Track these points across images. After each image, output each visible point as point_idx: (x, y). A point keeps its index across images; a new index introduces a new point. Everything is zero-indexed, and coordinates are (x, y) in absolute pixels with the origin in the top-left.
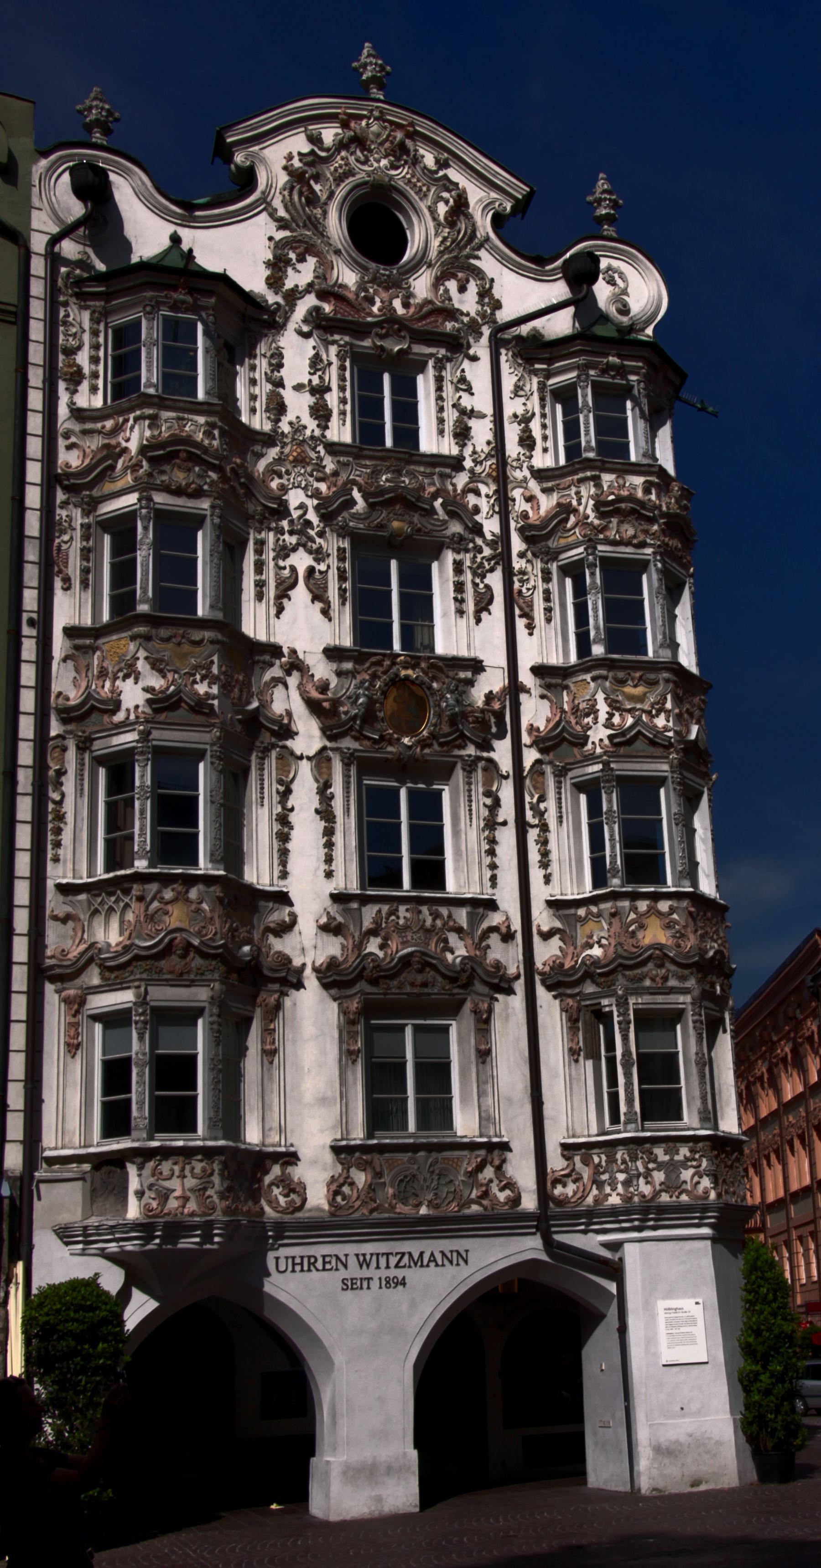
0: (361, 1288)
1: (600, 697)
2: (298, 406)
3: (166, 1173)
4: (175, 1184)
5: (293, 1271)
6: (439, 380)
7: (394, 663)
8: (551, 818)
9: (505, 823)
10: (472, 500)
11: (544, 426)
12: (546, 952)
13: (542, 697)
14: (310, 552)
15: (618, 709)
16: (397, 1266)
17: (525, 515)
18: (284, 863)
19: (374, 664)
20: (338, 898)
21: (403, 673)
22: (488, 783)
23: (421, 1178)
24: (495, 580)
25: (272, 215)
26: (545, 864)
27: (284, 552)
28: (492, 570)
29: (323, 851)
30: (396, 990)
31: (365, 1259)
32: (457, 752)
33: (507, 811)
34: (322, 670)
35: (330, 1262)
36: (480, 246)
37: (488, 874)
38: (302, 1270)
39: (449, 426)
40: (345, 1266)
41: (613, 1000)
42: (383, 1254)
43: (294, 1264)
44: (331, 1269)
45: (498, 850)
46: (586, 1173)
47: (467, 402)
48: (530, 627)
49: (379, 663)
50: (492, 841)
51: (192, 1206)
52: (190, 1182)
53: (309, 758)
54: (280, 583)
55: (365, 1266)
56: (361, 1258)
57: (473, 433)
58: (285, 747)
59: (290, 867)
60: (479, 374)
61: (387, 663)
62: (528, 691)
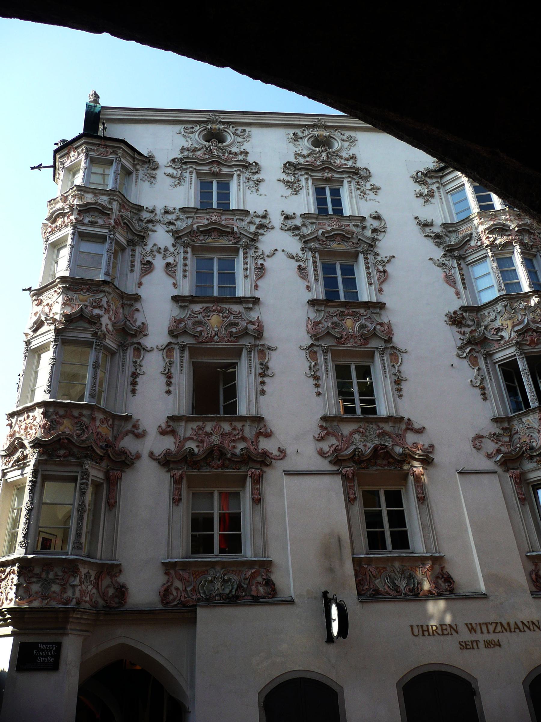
0: (473, 648)
5: (423, 635)
16: (494, 632)
31: (472, 628)
35: (446, 629)
38: (429, 635)
40: (457, 632)
42: (483, 623)
43: (423, 631)
44: (448, 634)
55: (473, 632)
56: (470, 627)
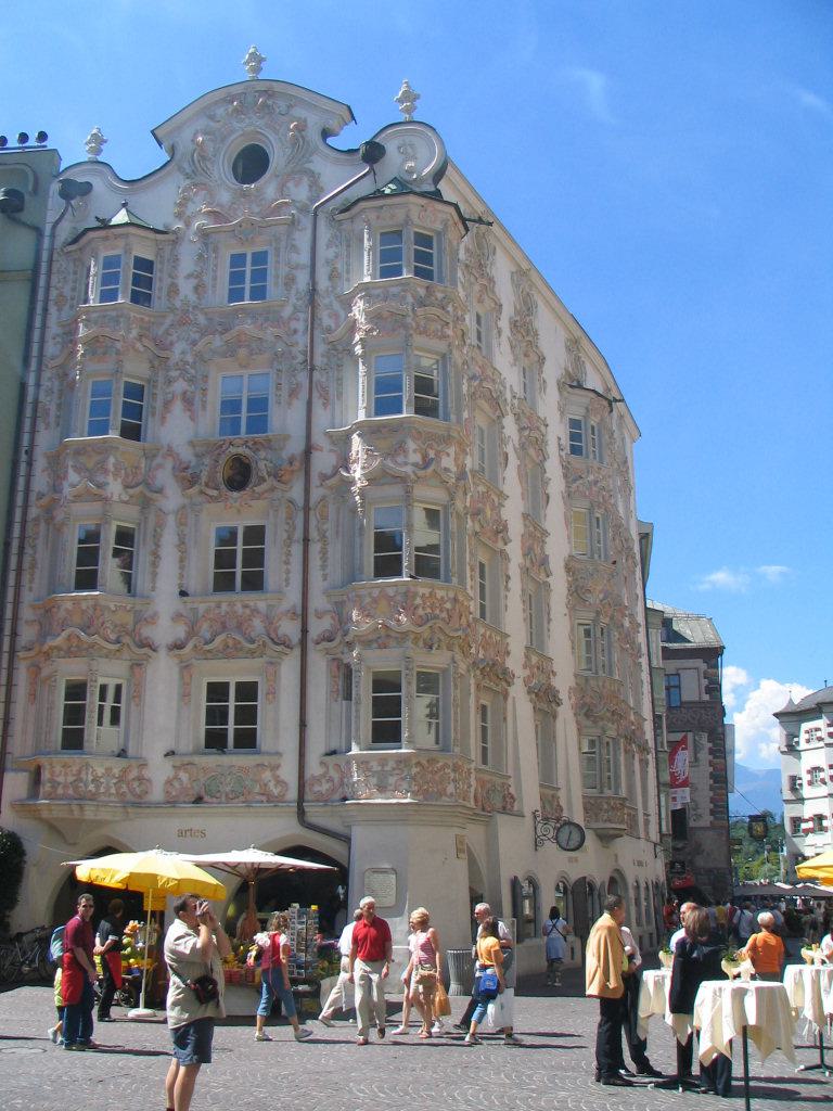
2: (186, 288)
3: (58, 772)
4: (61, 779)
10: (294, 325)
13: (331, 451)
17: (329, 330)
24: (302, 377)
25: (180, 169)
26: (323, 567)
27: (169, 382)
33: (299, 534)
36: (312, 154)
37: (285, 576)
51: (71, 792)
52: (71, 779)
59: (157, 585)
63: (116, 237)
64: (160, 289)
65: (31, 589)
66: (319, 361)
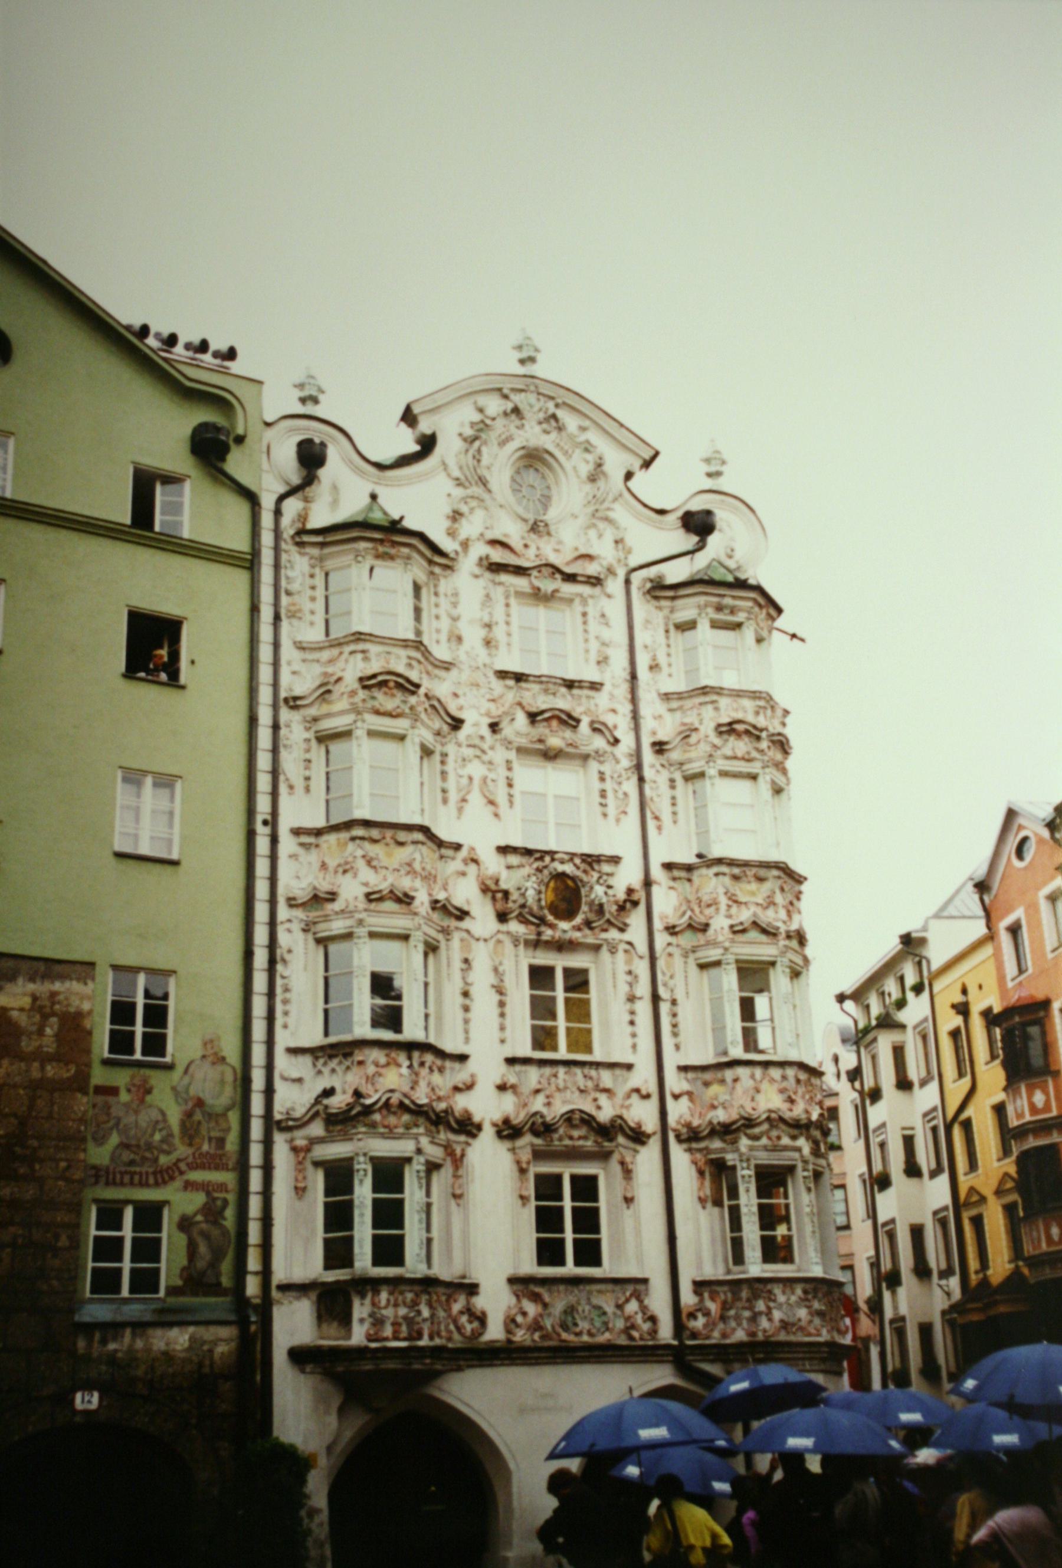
1: (721, 890)
3: (383, 1303)
6: (584, 614)
7: (553, 860)
8: (680, 996)
9: (640, 998)
11: (669, 655)
12: (678, 1111)
13: (671, 888)
14: (484, 763)
15: (736, 902)
18: (466, 1032)
19: (537, 859)
20: (511, 1061)
21: (560, 868)
22: (629, 962)
23: (580, 1309)
26: (675, 1035)
28: (628, 779)
29: (496, 1021)
30: (561, 1140)
32: (604, 935)
33: (643, 989)
34: (493, 865)
39: (593, 656)
41: (735, 1156)
45: (638, 1019)
46: (713, 1307)
47: (606, 634)
48: (659, 828)
49: (541, 859)
50: (632, 1013)
53: (485, 940)
54: (459, 790)
57: (612, 661)
58: (468, 931)
60: (615, 609)
61: (547, 859)
62: (659, 884)
63: (395, 544)
64: (438, 631)
65: (285, 1026)
66: (648, 773)
